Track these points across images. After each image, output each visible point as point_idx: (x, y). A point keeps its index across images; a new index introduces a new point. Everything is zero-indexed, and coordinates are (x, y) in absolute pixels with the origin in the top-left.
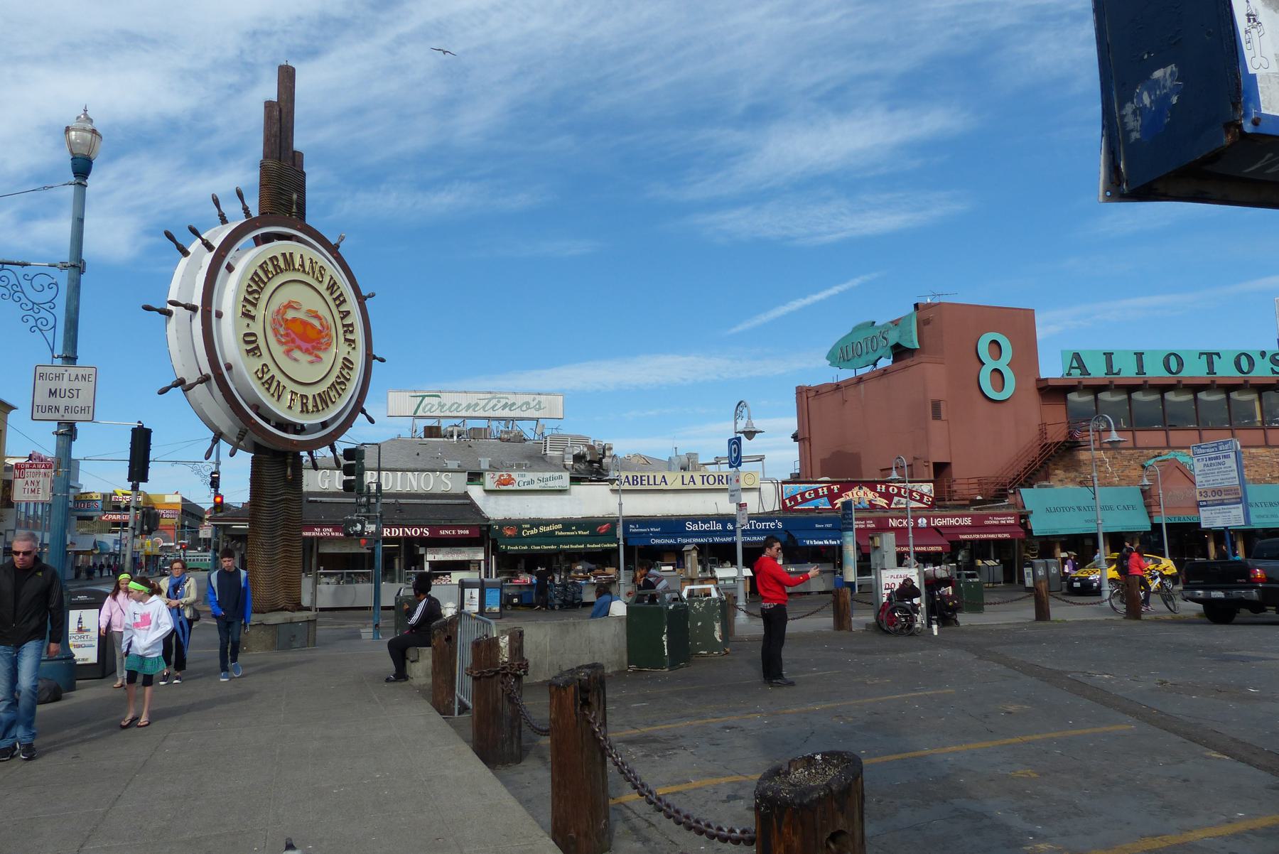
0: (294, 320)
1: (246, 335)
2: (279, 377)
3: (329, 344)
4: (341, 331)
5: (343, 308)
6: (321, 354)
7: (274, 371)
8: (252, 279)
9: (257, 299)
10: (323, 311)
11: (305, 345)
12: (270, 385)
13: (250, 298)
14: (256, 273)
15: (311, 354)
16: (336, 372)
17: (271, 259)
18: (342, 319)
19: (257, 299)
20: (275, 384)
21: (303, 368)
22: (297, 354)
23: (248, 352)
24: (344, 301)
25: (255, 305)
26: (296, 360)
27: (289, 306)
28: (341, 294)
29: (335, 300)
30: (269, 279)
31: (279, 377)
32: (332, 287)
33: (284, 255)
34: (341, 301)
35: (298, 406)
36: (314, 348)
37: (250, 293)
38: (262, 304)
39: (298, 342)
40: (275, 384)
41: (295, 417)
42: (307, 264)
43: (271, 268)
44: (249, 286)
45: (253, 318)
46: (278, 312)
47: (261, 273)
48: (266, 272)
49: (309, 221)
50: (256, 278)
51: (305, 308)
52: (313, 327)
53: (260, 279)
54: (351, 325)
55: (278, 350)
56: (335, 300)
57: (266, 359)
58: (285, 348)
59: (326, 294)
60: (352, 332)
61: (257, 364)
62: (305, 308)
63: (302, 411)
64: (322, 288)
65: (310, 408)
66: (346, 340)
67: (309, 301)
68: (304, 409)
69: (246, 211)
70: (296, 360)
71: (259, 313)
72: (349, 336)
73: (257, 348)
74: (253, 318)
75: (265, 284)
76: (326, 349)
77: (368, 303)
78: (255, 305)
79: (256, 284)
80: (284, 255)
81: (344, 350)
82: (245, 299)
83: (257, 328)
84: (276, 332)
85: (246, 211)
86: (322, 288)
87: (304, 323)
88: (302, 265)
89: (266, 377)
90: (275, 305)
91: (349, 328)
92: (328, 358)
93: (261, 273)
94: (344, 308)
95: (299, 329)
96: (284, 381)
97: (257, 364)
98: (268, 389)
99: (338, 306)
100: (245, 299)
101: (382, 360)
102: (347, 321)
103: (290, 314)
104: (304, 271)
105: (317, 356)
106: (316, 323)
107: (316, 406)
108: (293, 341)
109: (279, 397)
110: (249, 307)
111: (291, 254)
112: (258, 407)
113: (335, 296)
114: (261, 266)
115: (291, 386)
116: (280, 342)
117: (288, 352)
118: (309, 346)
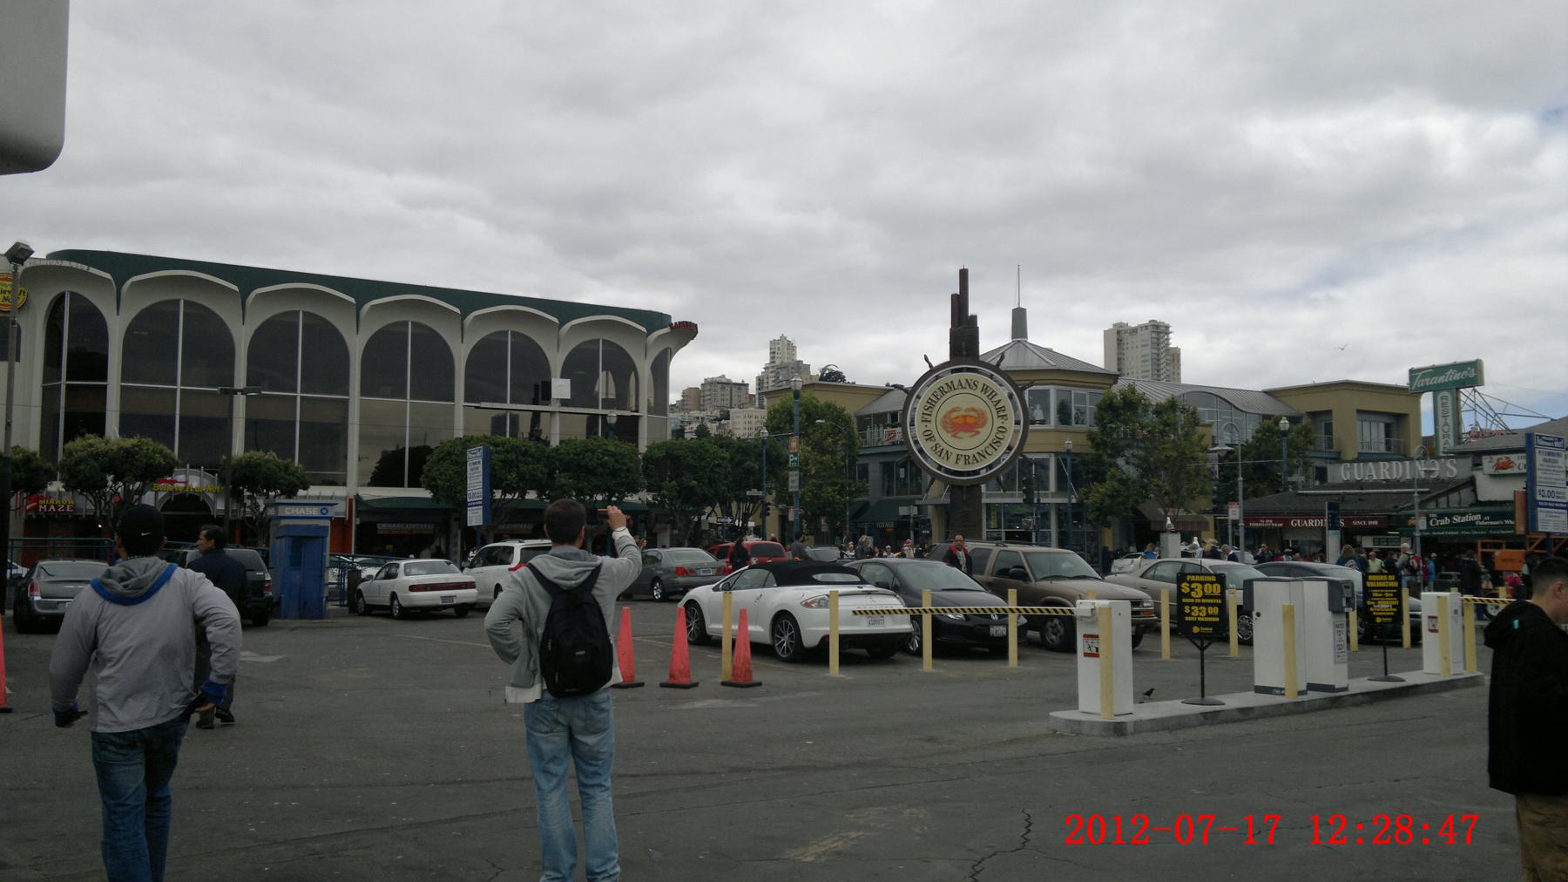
2: (947, 448)
10: (983, 406)
27: (954, 410)
32: (985, 389)
34: (993, 394)
35: (962, 461)
41: (960, 467)
55: (947, 437)
68: (967, 462)
71: (932, 418)
76: (983, 425)
79: (931, 404)
81: (998, 422)
83: (931, 426)
86: (978, 392)
91: (1002, 409)
92: (984, 431)
103: (954, 415)
115: (956, 452)
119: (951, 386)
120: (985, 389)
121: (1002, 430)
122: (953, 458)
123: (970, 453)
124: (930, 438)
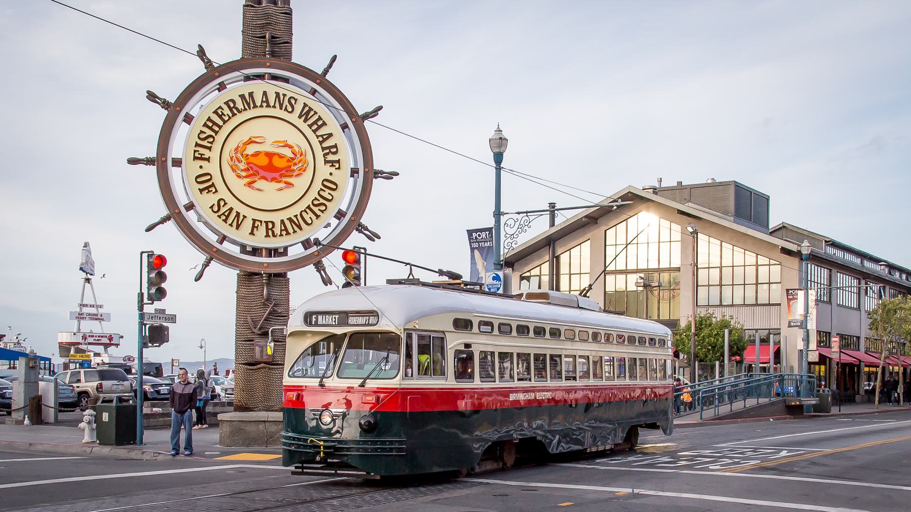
0: (256, 154)
1: (197, 177)
2: (238, 207)
5: (323, 131)
7: (232, 202)
9: (211, 143)
11: (270, 175)
14: (209, 119)
15: (280, 182)
16: (313, 194)
17: (226, 103)
20: (234, 214)
21: (269, 196)
23: (201, 191)
24: (324, 124)
27: (251, 142)
29: (310, 126)
30: (225, 122)
32: (306, 114)
33: (242, 97)
34: (319, 124)
35: (262, 230)
36: (281, 176)
38: (217, 147)
39: (262, 173)
40: (234, 214)
42: (272, 99)
43: (227, 111)
44: (202, 132)
45: (208, 160)
46: (236, 149)
50: (210, 124)
51: (270, 140)
52: (281, 156)
53: (214, 123)
54: (335, 146)
55: (238, 185)
57: (223, 193)
59: (300, 123)
61: (212, 199)
62: (270, 140)
63: (267, 236)
64: (294, 118)
65: (277, 231)
66: (326, 162)
67: (273, 133)
70: (259, 190)
71: (214, 155)
72: (331, 157)
73: (213, 185)
74: (208, 160)
75: (220, 127)
78: (210, 149)
80: (242, 97)
81: (324, 171)
83: (212, 168)
86: (294, 118)
87: (270, 155)
94: (323, 131)
95: (264, 161)
96: (243, 210)
97: (212, 199)
100: (197, 145)
102: (326, 144)
103: (251, 150)
104: (268, 106)
105: (286, 183)
106: (287, 152)
107: (286, 229)
109: (238, 227)
111: (251, 94)
113: (310, 122)
114: (215, 112)
115: (251, 214)
117: (250, 184)
118: (277, 175)
119: (249, 101)
120: (306, 114)
121: (330, 185)
122: (247, 225)
123: (276, 218)
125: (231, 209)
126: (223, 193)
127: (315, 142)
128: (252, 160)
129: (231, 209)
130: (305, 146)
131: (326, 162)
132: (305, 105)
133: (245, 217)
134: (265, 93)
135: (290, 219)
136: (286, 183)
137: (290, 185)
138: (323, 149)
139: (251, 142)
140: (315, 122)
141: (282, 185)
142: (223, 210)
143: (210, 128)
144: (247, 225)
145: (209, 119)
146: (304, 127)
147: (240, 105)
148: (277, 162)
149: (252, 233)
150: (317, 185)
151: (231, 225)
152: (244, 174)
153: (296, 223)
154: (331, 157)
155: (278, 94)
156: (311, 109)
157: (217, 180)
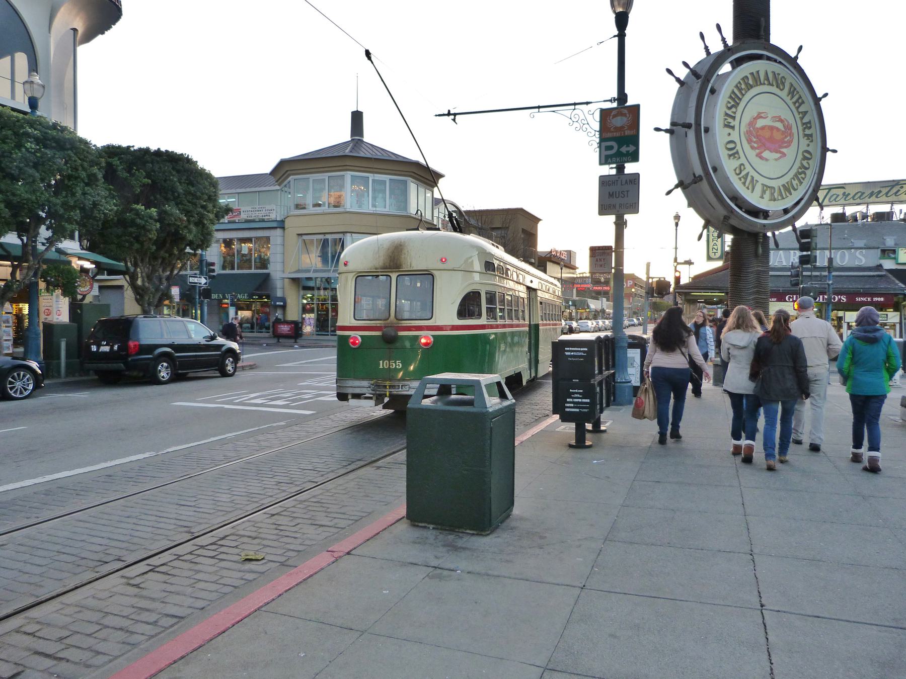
0: (763, 128)
2: (753, 173)
3: (789, 143)
4: (800, 128)
6: (784, 150)
8: (731, 97)
12: (746, 179)
13: (729, 112)
14: (733, 92)
16: (797, 164)
18: (802, 119)
19: (735, 113)
22: (766, 154)
23: (730, 156)
25: (734, 118)
26: (767, 160)
27: (759, 116)
28: (800, 97)
29: (795, 103)
30: (743, 95)
31: (753, 173)
35: (767, 195)
37: (730, 108)
38: (738, 118)
40: (749, 178)
42: (770, 76)
43: (743, 86)
45: (733, 128)
47: (736, 91)
48: (740, 90)
49: (774, 40)
51: (770, 116)
52: (778, 129)
55: (751, 154)
56: (795, 103)
58: (758, 151)
59: (788, 99)
60: (810, 128)
61: (735, 163)
62: (770, 116)
65: (776, 195)
69: (723, 40)
72: (808, 132)
73: (737, 152)
74: (733, 128)
75: (740, 99)
77: (823, 103)
78: (734, 118)
80: (752, 74)
82: (727, 114)
83: (735, 136)
84: (749, 141)
85: (723, 40)
86: (784, 94)
87: (772, 128)
88: (768, 79)
89: (743, 173)
90: (746, 119)
93: (736, 91)
94: (801, 109)
95: (767, 134)
97: (735, 163)
98: (744, 183)
99: (798, 108)
101: (835, 151)
103: (760, 123)
105: (781, 152)
106: (779, 125)
107: (781, 194)
108: (764, 145)
110: (730, 120)
111: (758, 72)
112: (737, 199)
113: (795, 99)
114: (736, 86)
116: (752, 148)
117: (759, 155)
120: (792, 92)
122: (758, 188)
124: (734, 155)
125: (748, 173)
126: (743, 160)
127: (798, 117)
128: (760, 132)
129: (748, 173)
130: (791, 121)
131: (806, 135)
132: (792, 85)
133: (757, 181)
134: (766, 73)
135: (783, 186)
136: (781, 152)
137: (784, 155)
138: (803, 124)
139: (759, 116)
140: (797, 101)
141: (778, 155)
142: (743, 173)
143: (734, 100)
144: (758, 188)
145: (733, 92)
146: (790, 103)
147: (751, 82)
148: (777, 136)
149: (762, 197)
150: (800, 157)
151: (748, 188)
152: (756, 145)
153: (788, 188)
154: (808, 132)
155: (774, 73)
156: (795, 89)
157: (739, 147)
